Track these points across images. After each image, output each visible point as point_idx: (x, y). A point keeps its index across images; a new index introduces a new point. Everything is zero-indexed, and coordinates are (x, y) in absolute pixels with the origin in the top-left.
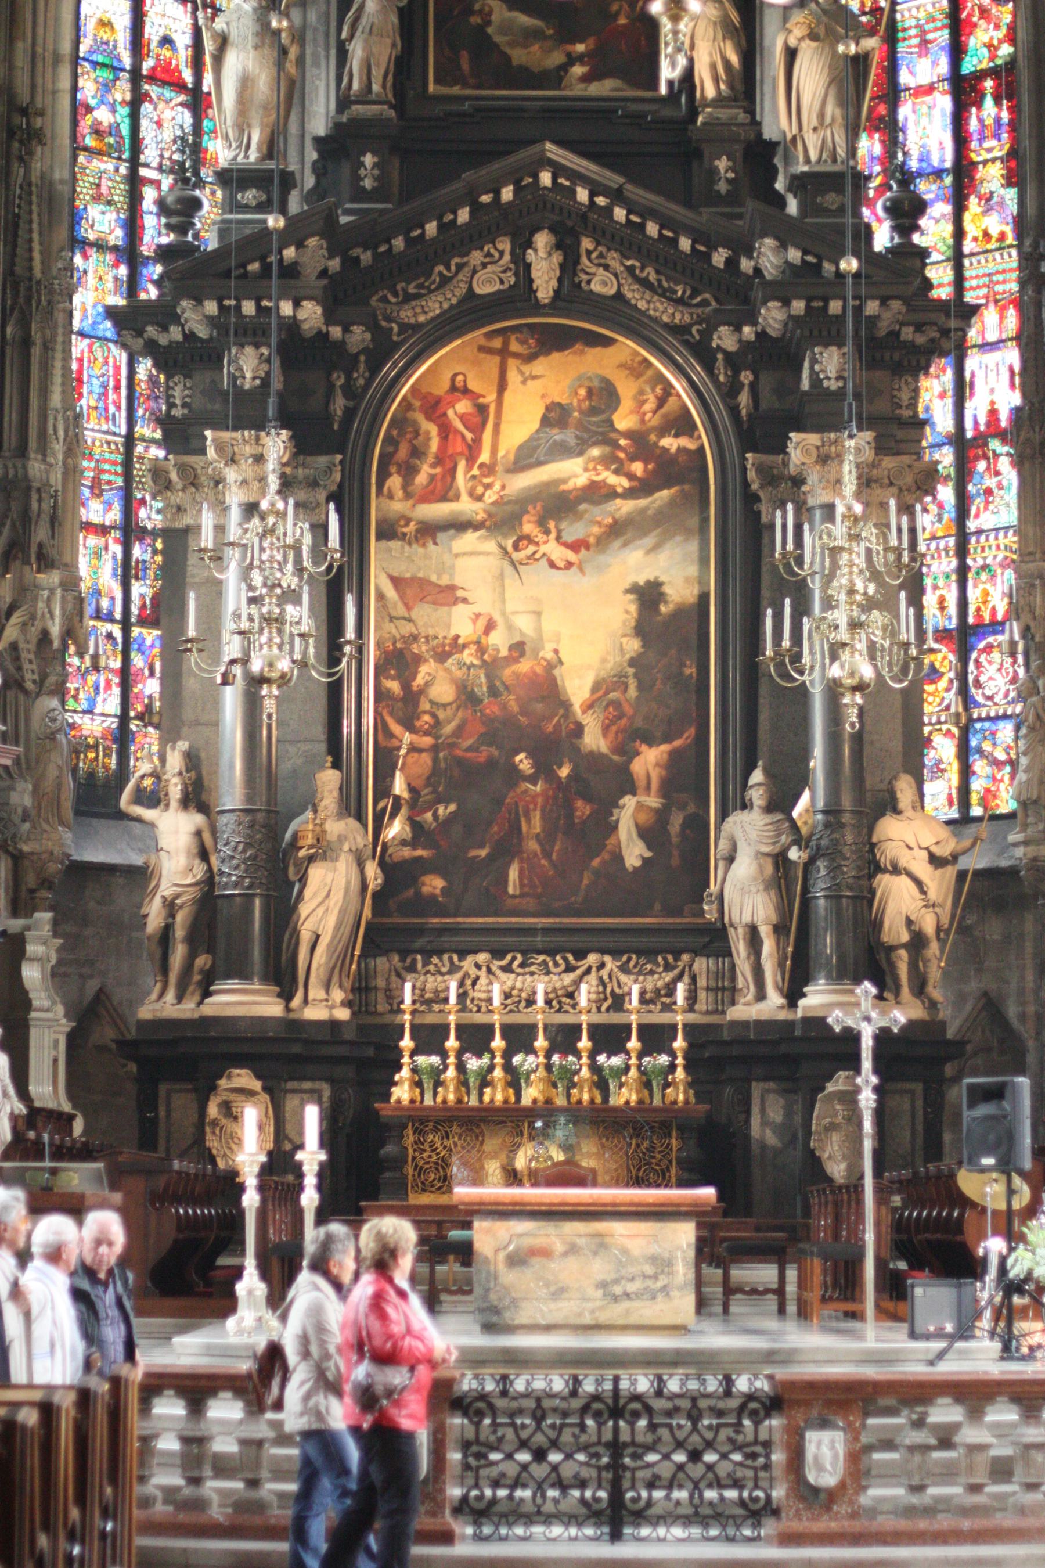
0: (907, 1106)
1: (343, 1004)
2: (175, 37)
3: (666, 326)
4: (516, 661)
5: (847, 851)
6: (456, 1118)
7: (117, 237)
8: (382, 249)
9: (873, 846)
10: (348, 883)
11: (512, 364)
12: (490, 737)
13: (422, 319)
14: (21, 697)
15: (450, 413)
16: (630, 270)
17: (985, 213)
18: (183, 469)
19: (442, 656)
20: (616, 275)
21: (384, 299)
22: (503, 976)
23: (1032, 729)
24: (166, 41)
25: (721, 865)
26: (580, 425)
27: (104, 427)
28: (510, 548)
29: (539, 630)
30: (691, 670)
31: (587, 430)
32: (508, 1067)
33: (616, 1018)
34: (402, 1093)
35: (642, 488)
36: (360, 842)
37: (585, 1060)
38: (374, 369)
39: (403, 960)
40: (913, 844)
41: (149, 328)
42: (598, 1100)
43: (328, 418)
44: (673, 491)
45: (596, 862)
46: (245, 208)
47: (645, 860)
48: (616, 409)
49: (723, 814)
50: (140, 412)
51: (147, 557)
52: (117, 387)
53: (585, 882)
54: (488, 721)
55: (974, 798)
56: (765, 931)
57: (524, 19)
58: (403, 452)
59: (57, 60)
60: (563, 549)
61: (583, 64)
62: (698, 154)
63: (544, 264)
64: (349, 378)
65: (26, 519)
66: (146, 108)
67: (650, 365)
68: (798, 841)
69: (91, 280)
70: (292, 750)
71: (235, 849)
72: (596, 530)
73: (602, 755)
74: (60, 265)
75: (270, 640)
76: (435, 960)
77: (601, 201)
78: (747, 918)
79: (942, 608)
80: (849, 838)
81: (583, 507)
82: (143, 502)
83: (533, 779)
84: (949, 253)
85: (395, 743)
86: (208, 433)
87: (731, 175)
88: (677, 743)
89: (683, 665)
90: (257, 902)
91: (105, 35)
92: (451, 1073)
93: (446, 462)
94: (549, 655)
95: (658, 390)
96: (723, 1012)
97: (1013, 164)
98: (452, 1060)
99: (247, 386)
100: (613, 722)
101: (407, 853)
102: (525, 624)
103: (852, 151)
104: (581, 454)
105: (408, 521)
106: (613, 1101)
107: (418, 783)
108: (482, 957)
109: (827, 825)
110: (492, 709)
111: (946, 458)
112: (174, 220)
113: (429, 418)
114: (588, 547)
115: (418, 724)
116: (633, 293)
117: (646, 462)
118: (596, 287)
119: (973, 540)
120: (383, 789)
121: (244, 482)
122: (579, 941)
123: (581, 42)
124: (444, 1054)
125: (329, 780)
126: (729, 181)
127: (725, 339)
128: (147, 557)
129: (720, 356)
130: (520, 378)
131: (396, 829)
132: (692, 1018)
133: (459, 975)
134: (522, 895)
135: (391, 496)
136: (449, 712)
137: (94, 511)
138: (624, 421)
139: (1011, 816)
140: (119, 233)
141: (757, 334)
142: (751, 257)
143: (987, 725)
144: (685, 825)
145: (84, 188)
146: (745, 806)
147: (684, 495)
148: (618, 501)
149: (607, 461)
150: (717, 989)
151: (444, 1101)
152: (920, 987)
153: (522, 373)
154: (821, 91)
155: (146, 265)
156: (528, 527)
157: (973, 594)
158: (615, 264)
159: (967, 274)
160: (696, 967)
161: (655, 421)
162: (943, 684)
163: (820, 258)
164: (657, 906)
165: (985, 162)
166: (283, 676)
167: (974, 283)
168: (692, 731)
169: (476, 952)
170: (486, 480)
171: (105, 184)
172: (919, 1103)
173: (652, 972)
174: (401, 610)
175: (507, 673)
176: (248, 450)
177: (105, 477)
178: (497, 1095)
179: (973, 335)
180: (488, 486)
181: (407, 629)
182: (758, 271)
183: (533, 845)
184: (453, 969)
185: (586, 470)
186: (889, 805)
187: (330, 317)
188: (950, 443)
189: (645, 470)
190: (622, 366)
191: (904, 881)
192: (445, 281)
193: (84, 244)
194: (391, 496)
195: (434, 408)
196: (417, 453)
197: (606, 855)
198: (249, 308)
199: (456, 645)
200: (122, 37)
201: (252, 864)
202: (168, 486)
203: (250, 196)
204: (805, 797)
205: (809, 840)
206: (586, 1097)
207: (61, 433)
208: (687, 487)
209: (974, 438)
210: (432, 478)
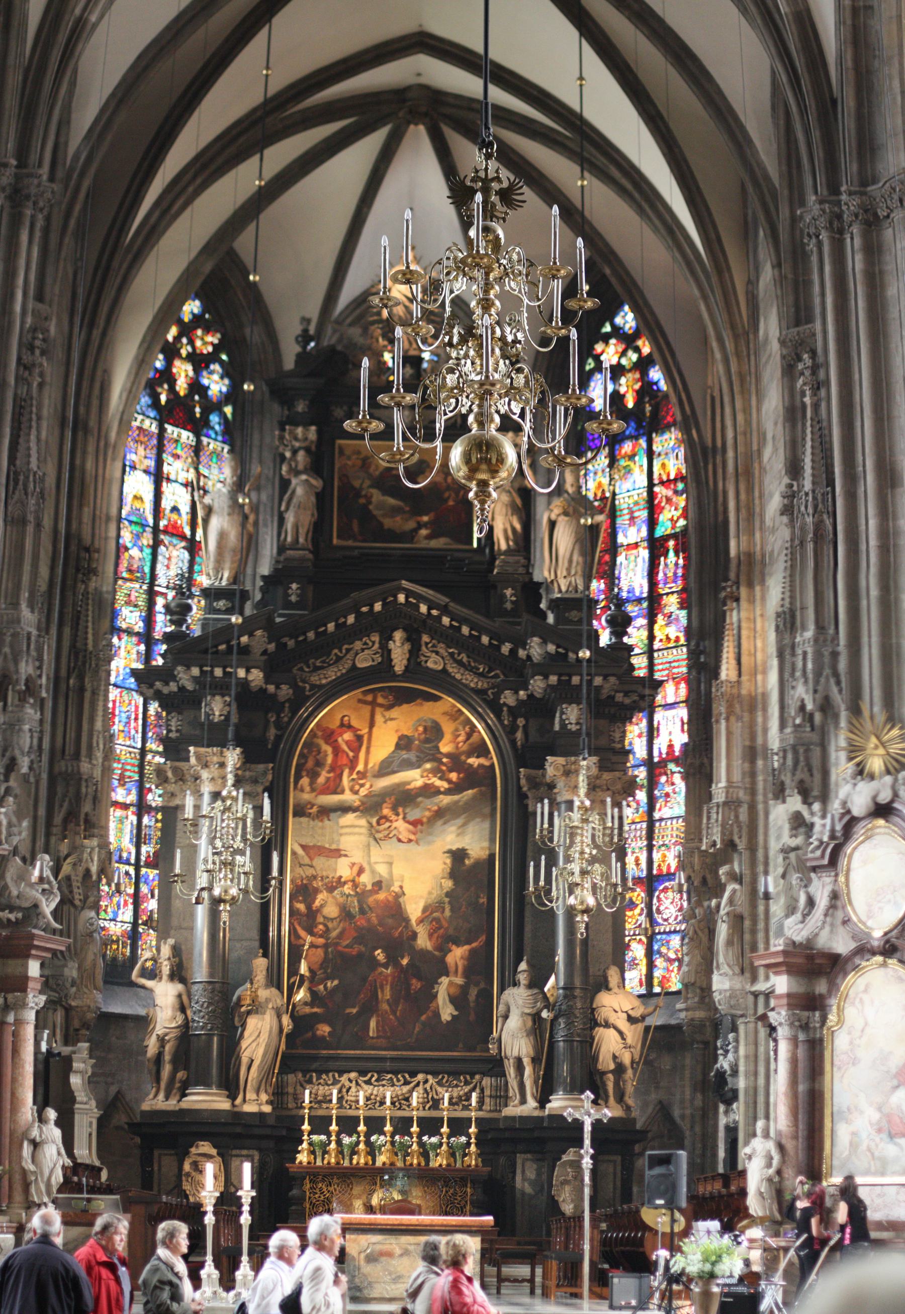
0: (611, 1170)
1: (267, 1102)
2: (180, 507)
3: (472, 689)
4: (377, 892)
5: (577, 1012)
6: (336, 1174)
7: (139, 627)
8: (301, 638)
9: (593, 1010)
10: (271, 1028)
11: (378, 710)
12: (360, 939)
13: (324, 681)
15: (340, 739)
16: (452, 655)
17: (667, 625)
18: (175, 770)
19: (331, 889)
20: (443, 658)
21: (301, 669)
22: (366, 1087)
23: (691, 939)
24: (175, 509)
25: (500, 1020)
26: (419, 750)
27: (128, 743)
28: (374, 823)
29: (391, 873)
30: (483, 900)
31: (422, 752)
32: (368, 1143)
33: (434, 1114)
34: (303, 1158)
35: (456, 788)
36: (279, 1002)
37: (415, 1139)
38: (294, 712)
39: (304, 1076)
40: (618, 1009)
41: (157, 683)
42: (423, 1164)
43: (264, 740)
45: (423, 1018)
46: (218, 611)
47: (453, 1016)
48: (441, 740)
49: (502, 989)
50: (150, 734)
51: (152, 823)
52: (136, 719)
53: (417, 1029)
54: (358, 929)
55: (656, 982)
56: (526, 1061)
57: (391, 501)
58: (310, 764)
59: (108, 519)
60: (407, 825)
61: (427, 528)
62: (494, 587)
63: (399, 650)
64: (278, 717)
65: (78, 798)
66: (162, 549)
67: (462, 713)
68: (548, 1006)
69: (122, 653)
70: (238, 945)
71: (202, 1006)
72: (427, 814)
73: (428, 952)
74: (104, 643)
75: (226, 876)
76: (324, 1076)
77: (435, 612)
78: (515, 1053)
79: (637, 864)
80: (579, 1005)
81: (420, 799)
82: (150, 790)
83: (386, 966)
84: (645, 649)
85: (301, 942)
86: (192, 749)
87: (514, 599)
88: (474, 945)
89: (478, 897)
90: (215, 1039)
91: (138, 504)
92: (333, 1146)
93: (337, 770)
94: (397, 889)
95: (467, 729)
96: (500, 1111)
97: (684, 596)
98: (333, 1138)
99: (216, 720)
100: (435, 931)
101: (307, 1010)
102: (382, 870)
103: (587, 587)
104: (419, 767)
105: (313, 805)
106: (432, 1164)
107: (315, 967)
108: (353, 1075)
109: (565, 996)
110: (361, 922)
111: (642, 774)
112: (175, 617)
113: (327, 743)
114: (422, 824)
115: (316, 930)
116: (452, 669)
117: (459, 773)
118: (430, 665)
119: (657, 824)
120: (294, 970)
121: (213, 779)
122: (413, 1066)
124: (329, 1135)
125: (260, 964)
126: (512, 602)
127: (508, 698)
128: (152, 823)
129: (505, 709)
130: (383, 720)
131: (301, 995)
132: (481, 1114)
133: (339, 1086)
134: (377, 1038)
135: (302, 790)
136: (335, 923)
137: (120, 795)
138: (445, 747)
139: (678, 993)
140: (141, 624)
141: (528, 696)
142: (525, 649)
143: (664, 936)
144: (477, 996)
145: (120, 597)
146: (515, 984)
147: (482, 794)
148: (441, 796)
149: (435, 772)
150: (496, 1097)
151: (329, 1163)
152: (620, 1098)
153: (384, 716)
155: (156, 644)
156: (386, 811)
157: (656, 856)
158: (442, 651)
159: (656, 662)
160: (484, 1083)
161: (464, 747)
162: (637, 911)
163: (567, 650)
164: (461, 1045)
165: (667, 594)
166: (233, 898)
167: (660, 667)
168: (483, 938)
169: (349, 1072)
170: (361, 782)
171: (134, 594)
172: (619, 1168)
173: (457, 1086)
174: (307, 860)
175: (371, 900)
176: (215, 759)
177: (128, 774)
178: (361, 1160)
179: (659, 699)
180: (362, 786)
181: (310, 872)
182: (529, 657)
183: (385, 1007)
184: (335, 1082)
185: (422, 777)
186: (603, 985)
187: (268, 679)
188: (643, 765)
189: (458, 778)
190: (445, 713)
191: (612, 1031)
192: (339, 659)
193: (119, 631)
194: (302, 790)
195: (330, 736)
196: (319, 764)
197: (429, 1013)
198: (218, 672)
199: (340, 882)
200: (148, 507)
201: (212, 1015)
202: (166, 780)
203: (221, 604)
204: (552, 979)
205: (554, 1005)
206: (415, 1161)
207: (101, 746)
208: (483, 788)
209: (659, 762)
210: (328, 779)
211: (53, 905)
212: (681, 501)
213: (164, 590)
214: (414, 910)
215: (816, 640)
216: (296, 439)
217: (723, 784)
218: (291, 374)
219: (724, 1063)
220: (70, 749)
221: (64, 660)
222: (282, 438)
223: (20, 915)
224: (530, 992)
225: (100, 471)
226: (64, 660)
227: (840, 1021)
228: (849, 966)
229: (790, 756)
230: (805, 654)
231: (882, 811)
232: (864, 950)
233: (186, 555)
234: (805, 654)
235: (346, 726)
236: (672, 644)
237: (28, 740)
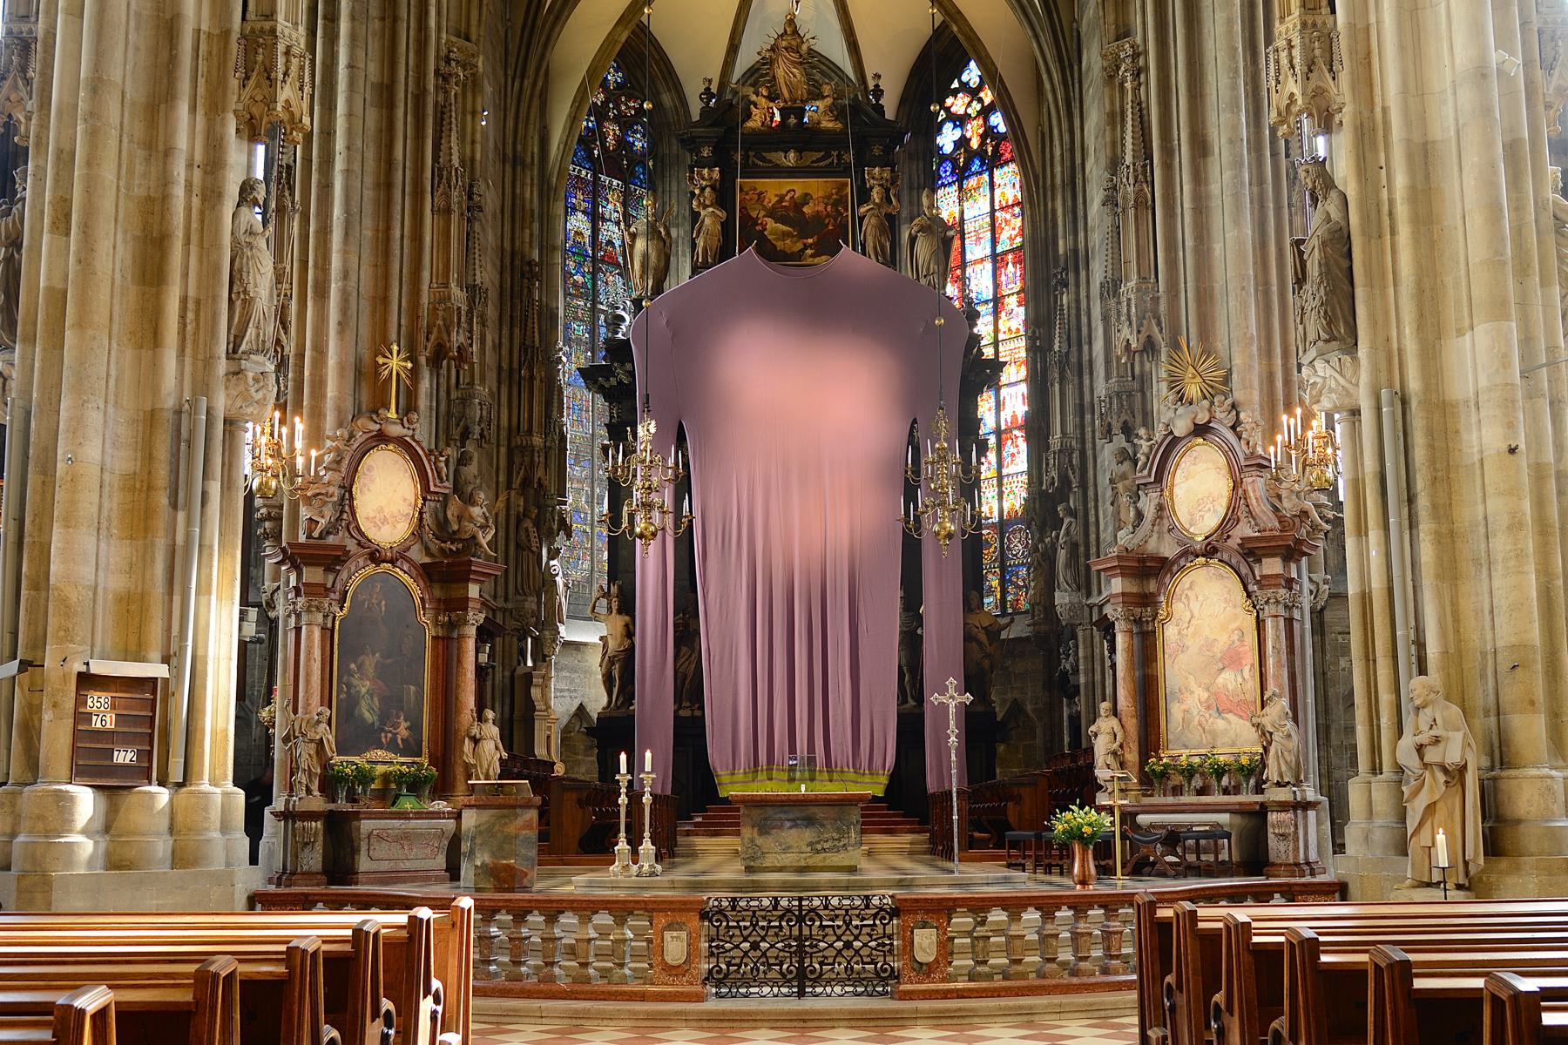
14: (531, 555)
24: (610, 243)
59: (554, 248)
111: (992, 440)
139: (1026, 612)
154: (928, 257)
162: (992, 550)
165: (1009, 295)
211: (489, 537)
212: (1018, 222)
213: (604, 308)
215: (1138, 290)
216: (703, 179)
217: (1059, 435)
218: (696, 125)
219: (1067, 665)
220: (524, 426)
221: (516, 355)
222: (692, 179)
223: (460, 546)
225: (545, 210)
226: (516, 355)
227: (1169, 616)
228: (1175, 568)
229: (1115, 401)
230: (1129, 300)
232: (1188, 553)
233: (620, 281)
234: (1129, 300)
236: (1013, 335)
237: (478, 412)
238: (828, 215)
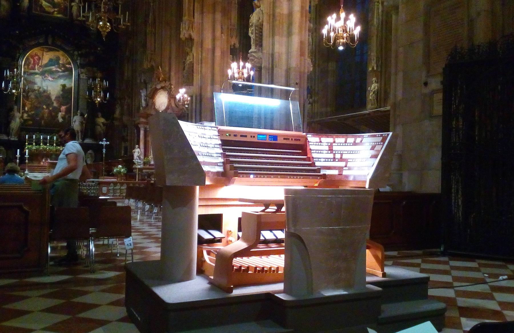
15: (35, 58)
35: (64, 71)
44: (68, 72)
49: (73, 117)
56: (79, 131)
58: (27, 62)
83: (46, 109)
93: (34, 64)
102: (45, 88)
123: (57, 9)
138: (61, 62)
146: (77, 115)
148: (60, 73)
168: (69, 105)
175: (43, 94)
180: (41, 69)
196: (30, 63)
210: (32, 67)
214: (53, 98)
224: (81, 117)
231: (163, 88)
235: (36, 55)
238: (62, 3)
